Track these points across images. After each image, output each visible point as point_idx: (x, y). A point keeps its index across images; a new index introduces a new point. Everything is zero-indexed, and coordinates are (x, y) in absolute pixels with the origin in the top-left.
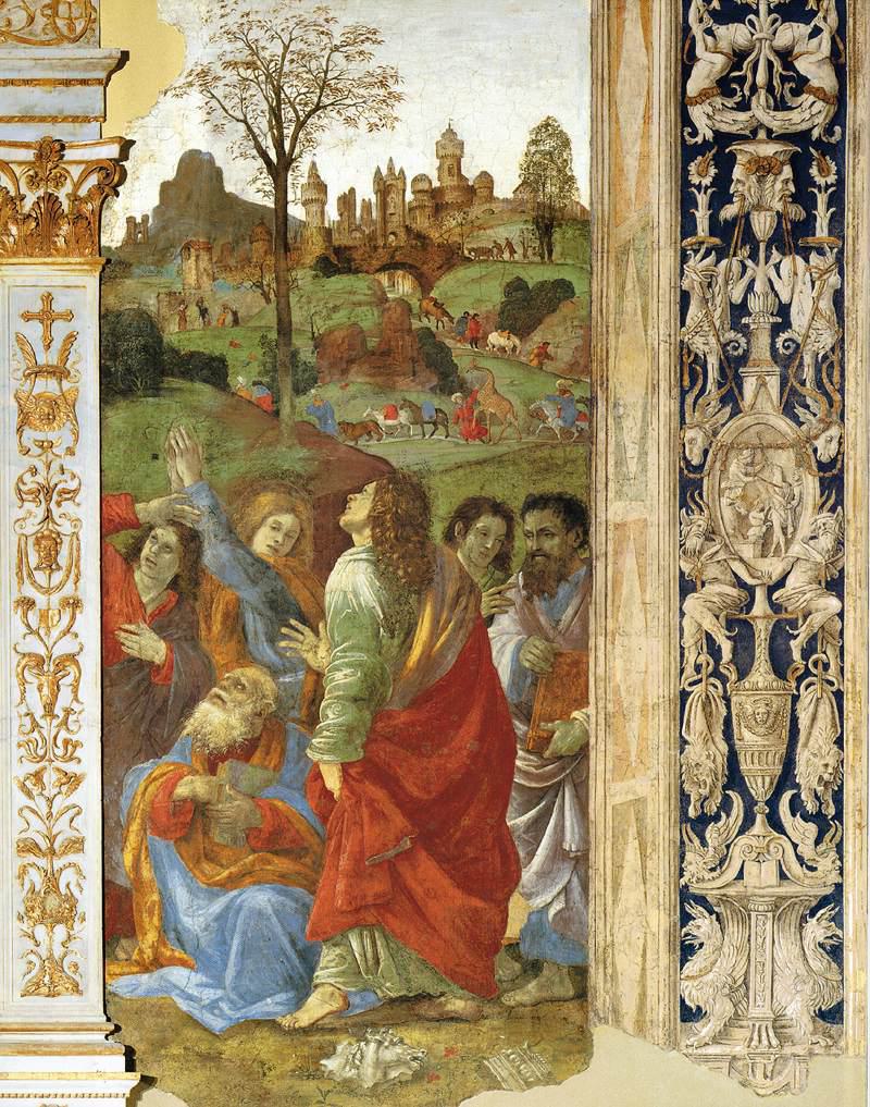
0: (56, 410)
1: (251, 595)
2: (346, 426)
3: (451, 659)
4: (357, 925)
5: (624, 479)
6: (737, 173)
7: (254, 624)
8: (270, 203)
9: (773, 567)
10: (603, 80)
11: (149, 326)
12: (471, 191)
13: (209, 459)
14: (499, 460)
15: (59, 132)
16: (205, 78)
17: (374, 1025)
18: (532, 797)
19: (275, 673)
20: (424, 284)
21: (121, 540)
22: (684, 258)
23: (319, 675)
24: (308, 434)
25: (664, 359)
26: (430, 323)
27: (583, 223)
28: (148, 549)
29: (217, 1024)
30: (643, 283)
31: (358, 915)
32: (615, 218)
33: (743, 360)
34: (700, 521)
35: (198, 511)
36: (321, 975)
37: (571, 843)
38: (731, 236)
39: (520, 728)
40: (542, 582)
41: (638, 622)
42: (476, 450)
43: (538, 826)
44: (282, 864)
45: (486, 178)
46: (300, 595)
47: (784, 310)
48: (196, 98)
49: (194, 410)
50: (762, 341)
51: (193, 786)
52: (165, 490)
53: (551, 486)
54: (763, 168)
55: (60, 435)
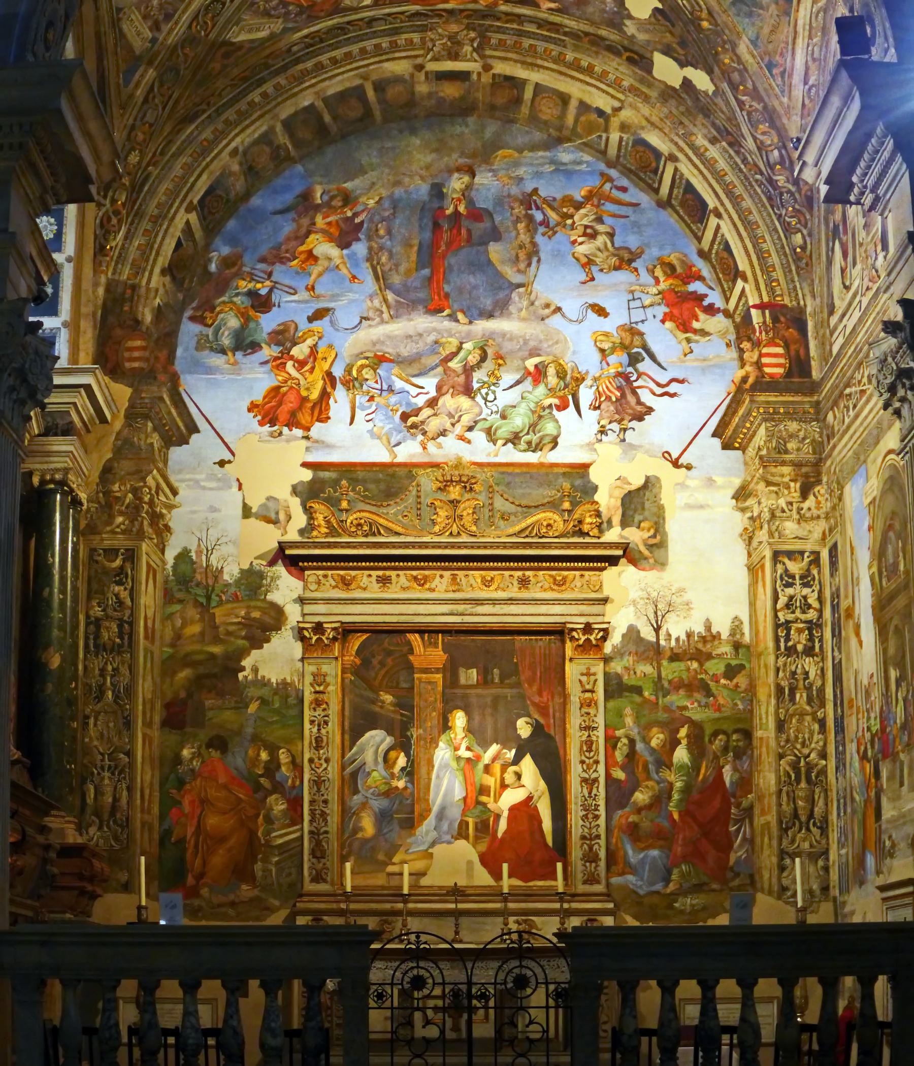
0: (590, 703)
1: (650, 759)
2: (678, 707)
3: (711, 779)
5: (761, 724)
6: (792, 632)
7: (651, 767)
8: (654, 640)
9: (806, 751)
10: (752, 605)
11: (619, 677)
13: (637, 717)
14: (725, 718)
15: (591, 620)
16: (634, 603)
17: (690, 893)
18: (736, 822)
19: (658, 783)
20: (701, 665)
21: (612, 741)
22: (777, 658)
23: (671, 785)
24: (667, 709)
25: (772, 688)
26: (703, 676)
27: (748, 647)
28: (619, 745)
29: (642, 892)
30: (766, 666)
31: (685, 859)
33: (796, 688)
34: (784, 736)
35: (634, 733)
36: (673, 877)
37: (748, 836)
38: (791, 651)
39: (733, 800)
40: (738, 755)
41: (767, 767)
42: (717, 715)
43: (738, 830)
44: (661, 843)
45: (719, 633)
47: (807, 673)
48: (632, 608)
49: (632, 702)
50: (801, 682)
52: (624, 726)
53: (740, 726)
54: (800, 631)
55: (592, 711)
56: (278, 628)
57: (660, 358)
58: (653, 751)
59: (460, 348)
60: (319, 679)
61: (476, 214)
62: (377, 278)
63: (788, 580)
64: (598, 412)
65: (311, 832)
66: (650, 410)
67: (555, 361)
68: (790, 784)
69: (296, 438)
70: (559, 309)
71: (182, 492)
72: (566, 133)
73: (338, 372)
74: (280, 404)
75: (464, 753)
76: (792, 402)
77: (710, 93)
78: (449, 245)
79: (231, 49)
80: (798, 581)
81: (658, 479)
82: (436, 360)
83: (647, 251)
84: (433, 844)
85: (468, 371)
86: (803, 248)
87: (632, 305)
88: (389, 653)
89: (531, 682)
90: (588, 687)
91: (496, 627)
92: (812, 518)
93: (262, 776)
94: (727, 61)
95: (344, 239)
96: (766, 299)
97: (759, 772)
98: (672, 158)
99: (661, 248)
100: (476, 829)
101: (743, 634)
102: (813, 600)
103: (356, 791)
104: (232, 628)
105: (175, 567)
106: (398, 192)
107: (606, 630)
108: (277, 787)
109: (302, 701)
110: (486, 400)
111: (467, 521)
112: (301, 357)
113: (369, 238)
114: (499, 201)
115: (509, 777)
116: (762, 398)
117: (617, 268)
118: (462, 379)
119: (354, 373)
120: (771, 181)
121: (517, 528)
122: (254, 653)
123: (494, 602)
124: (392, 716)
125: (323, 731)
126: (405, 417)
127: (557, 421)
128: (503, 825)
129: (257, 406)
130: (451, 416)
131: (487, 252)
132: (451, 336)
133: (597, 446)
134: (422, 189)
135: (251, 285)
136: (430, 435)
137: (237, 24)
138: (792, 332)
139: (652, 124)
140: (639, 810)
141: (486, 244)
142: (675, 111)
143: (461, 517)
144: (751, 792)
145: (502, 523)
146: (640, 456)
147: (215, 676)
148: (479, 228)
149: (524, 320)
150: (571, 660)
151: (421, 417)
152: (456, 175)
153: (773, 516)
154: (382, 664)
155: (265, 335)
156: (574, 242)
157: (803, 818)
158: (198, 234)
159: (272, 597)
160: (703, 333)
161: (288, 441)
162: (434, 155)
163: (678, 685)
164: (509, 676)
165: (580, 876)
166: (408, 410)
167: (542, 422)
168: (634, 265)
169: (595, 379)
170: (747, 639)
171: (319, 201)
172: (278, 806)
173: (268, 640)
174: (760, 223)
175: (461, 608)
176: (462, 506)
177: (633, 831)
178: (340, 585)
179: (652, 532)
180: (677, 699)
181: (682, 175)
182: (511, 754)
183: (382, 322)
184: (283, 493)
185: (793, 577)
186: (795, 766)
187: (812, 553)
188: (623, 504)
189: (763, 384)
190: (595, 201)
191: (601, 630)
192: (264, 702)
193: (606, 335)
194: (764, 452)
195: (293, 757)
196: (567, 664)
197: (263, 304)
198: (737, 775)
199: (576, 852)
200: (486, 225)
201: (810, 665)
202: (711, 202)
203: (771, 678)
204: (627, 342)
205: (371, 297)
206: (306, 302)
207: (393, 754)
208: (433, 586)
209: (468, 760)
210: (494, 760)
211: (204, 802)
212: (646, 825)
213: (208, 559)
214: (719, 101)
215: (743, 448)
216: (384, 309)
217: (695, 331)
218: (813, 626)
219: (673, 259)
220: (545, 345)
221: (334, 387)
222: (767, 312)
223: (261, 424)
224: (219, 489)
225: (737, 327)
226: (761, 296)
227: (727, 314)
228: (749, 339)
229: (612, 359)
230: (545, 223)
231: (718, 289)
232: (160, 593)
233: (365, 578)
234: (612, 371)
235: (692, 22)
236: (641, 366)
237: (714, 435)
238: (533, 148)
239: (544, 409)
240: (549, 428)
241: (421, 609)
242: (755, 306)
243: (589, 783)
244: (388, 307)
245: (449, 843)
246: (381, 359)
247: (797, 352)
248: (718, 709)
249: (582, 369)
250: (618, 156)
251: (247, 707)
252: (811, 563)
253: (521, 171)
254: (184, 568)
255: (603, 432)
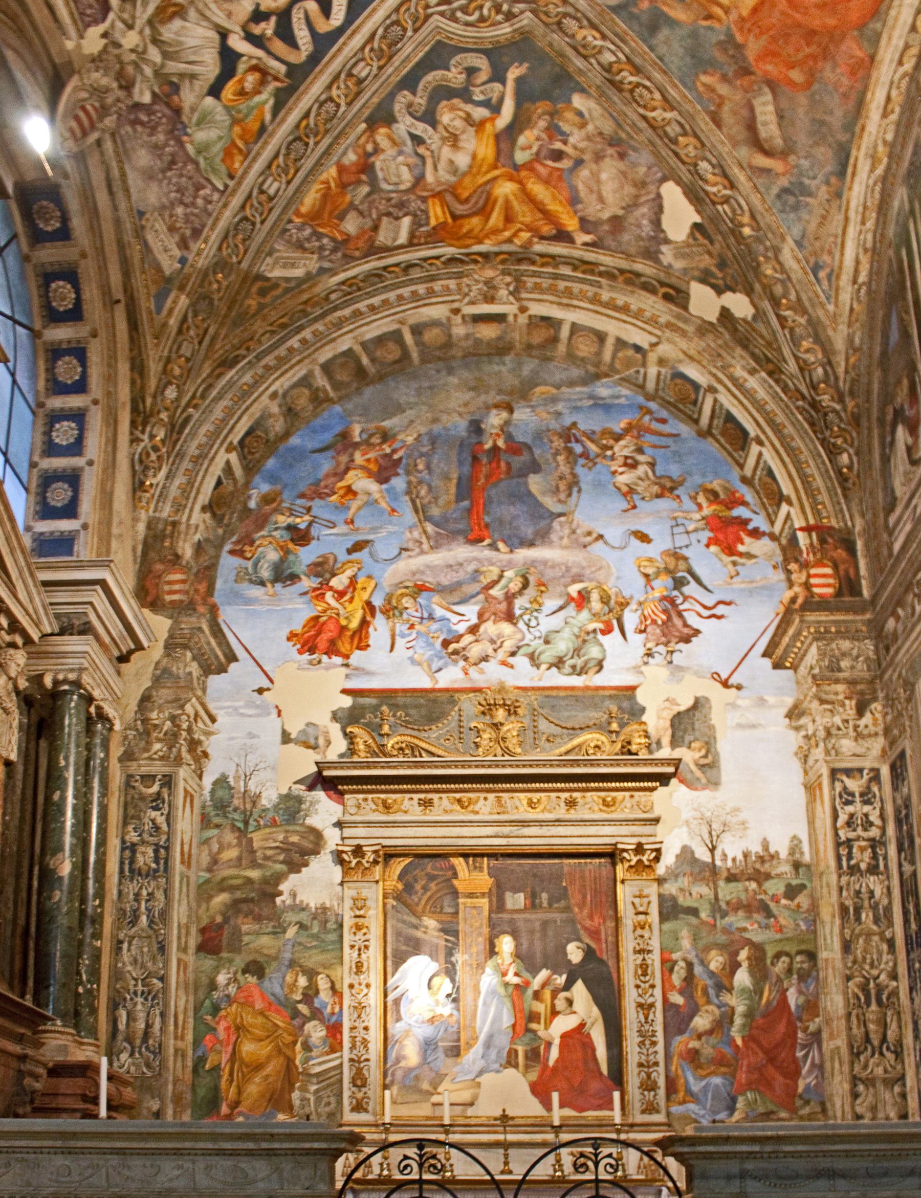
1: (709, 982)
4: (751, 1089)
7: (711, 992)
10: (811, 822)
11: (674, 899)
12: (772, 857)
14: (788, 939)
15: (643, 840)
16: (687, 823)
19: (719, 1007)
20: (760, 885)
21: (668, 965)
22: (840, 876)
23: (733, 1009)
24: (726, 931)
26: (762, 897)
27: (808, 867)
32: (818, 865)
33: (861, 907)
34: (851, 958)
38: (854, 870)
40: (803, 977)
42: (778, 936)
44: (723, 1069)
46: (726, 982)
48: (685, 829)
49: (689, 925)
51: (694, 1044)
53: (803, 947)
54: (862, 849)
56: (316, 852)
57: (705, 581)
58: (712, 974)
59: (501, 577)
60: (359, 904)
61: (515, 448)
62: (416, 511)
63: (847, 798)
64: (643, 635)
65: (351, 1060)
66: (697, 632)
67: (599, 587)
68: (860, 1006)
69: (335, 666)
70: (601, 537)
71: (220, 719)
72: (604, 369)
73: (378, 601)
74: (319, 633)
75: (511, 978)
76: (844, 621)
77: (749, 318)
78: (488, 477)
79: (267, 286)
80: (858, 799)
81: (707, 699)
82: (476, 587)
83: (689, 479)
84: (481, 1073)
85: (510, 598)
86: (850, 468)
87: (676, 530)
88: (432, 878)
89: (581, 906)
90: (641, 909)
91: (543, 849)
92: (870, 735)
93: (300, 1002)
94: (769, 272)
95: (383, 473)
96: (812, 521)
97: (826, 994)
98: (711, 390)
99: (704, 475)
100: (527, 1057)
101: (802, 853)
102: (874, 818)
103: (399, 1019)
104: (269, 853)
105: (213, 792)
106: (437, 428)
107: (658, 851)
108: (316, 1014)
109: (341, 926)
110: (528, 626)
111: (512, 743)
112: (340, 588)
113: (408, 473)
114: (539, 435)
115: (560, 1004)
116: (811, 617)
117: (658, 496)
118: (503, 606)
119: (394, 603)
120: (814, 405)
121: (563, 749)
122: (293, 877)
123: (541, 823)
124: (435, 941)
125: (364, 956)
126: (446, 644)
127: (601, 645)
128: (554, 1053)
129: (296, 635)
130: (493, 642)
131: (526, 484)
132: (492, 564)
133: (644, 668)
134: (460, 425)
135: (290, 520)
136: (472, 660)
137: (270, 254)
138: (841, 553)
139: (691, 358)
140: (699, 1037)
141: (526, 475)
142: (712, 344)
143: (504, 739)
144: (818, 1016)
145: (548, 745)
146: (688, 678)
147: (252, 900)
148: (517, 461)
149: (566, 547)
150: (623, 882)
151: (462, 644)
152: (494, 411)
153: (829, 733)
154: (425, 888)
155: (304, 568)
156: (614, 473)
157: (876, 1043)
158: (238, 472)
159: (311, 821)
160: (749, 556)
161: (327, 669)
162: (472, 394)
163: (737, 906)
164: (558, 901)
165: (637, 1106)
166: (449, 637)
167: (587, 645)
168: (676, 492)
169: (640, 604)
170: (807, 858)
171: (357, 439)
172: (316, 1032)
173: (306, 865)
174: (803, 448)
175: (506, 830)
176: (505, 728)
177: (693, 1057)
178: (381, 808)
179: (703, 752)
180: (737, 920)
181: (721, 406)
182: (561, 980)
183: (423, 552)
184: (323, 719)
185: (853, 795)
186: (864, 988)
187: (872, 770)
188: (672, 725)
189: (812, 604)
190: (635, 432)
191: (653, 850)
192: (302, 926)
193: (650, 560)
194: (816, 671)
195: (333, 983)
196: (619, 887)
197: (301, 537)
198: (802, 1000)
199: (633, 1078)
200: (525, 457)
201: (874, 883)
202: (752, 430)
203: (834, 898)
204: (671, 567)
205: (411, 529)
206: (346, 535)
207: (436, 981)
208: (477, 808)
209: (517, 986)
210: (544, 985)
211: (240, 1028)
212: (708, 1051)
213: (246, 785)
214: (761, 327)
215: (795, 667)
216: (424, 540)
217: (741, 555)
218: (874, 844)
219: (716, 485)
220: (587, 572)
221: (373, 615)
222: (814, 535)
223: (300, 652)
224: (257, 716)
225: (783, 549)
226: (806, 519)
227: (773, 537)
228: (797, 561)
229: (656, 583)
230: (585, 455)
231: (763, 513)
232: (197, 818)
233: (406, 802)
234: (657, 594)
235: (733, 231)
236: (686, 590)
237: (765, 655)
238: (571, 384)
239: (588, 633)
240: (594, 652)
241: (465, 831)
242: (801, 529)
243: (645, 1008)
244: (428, 538)
245: (498, 1072)
246: (421, 588)
247: (847, 572)
248: (780, 930)
249: (626, 594)
250: (657, 390)
251: (284, 932)
252: (870, 780)
253: (560, 407)
254: (220, 793)
255: (649, 654)
